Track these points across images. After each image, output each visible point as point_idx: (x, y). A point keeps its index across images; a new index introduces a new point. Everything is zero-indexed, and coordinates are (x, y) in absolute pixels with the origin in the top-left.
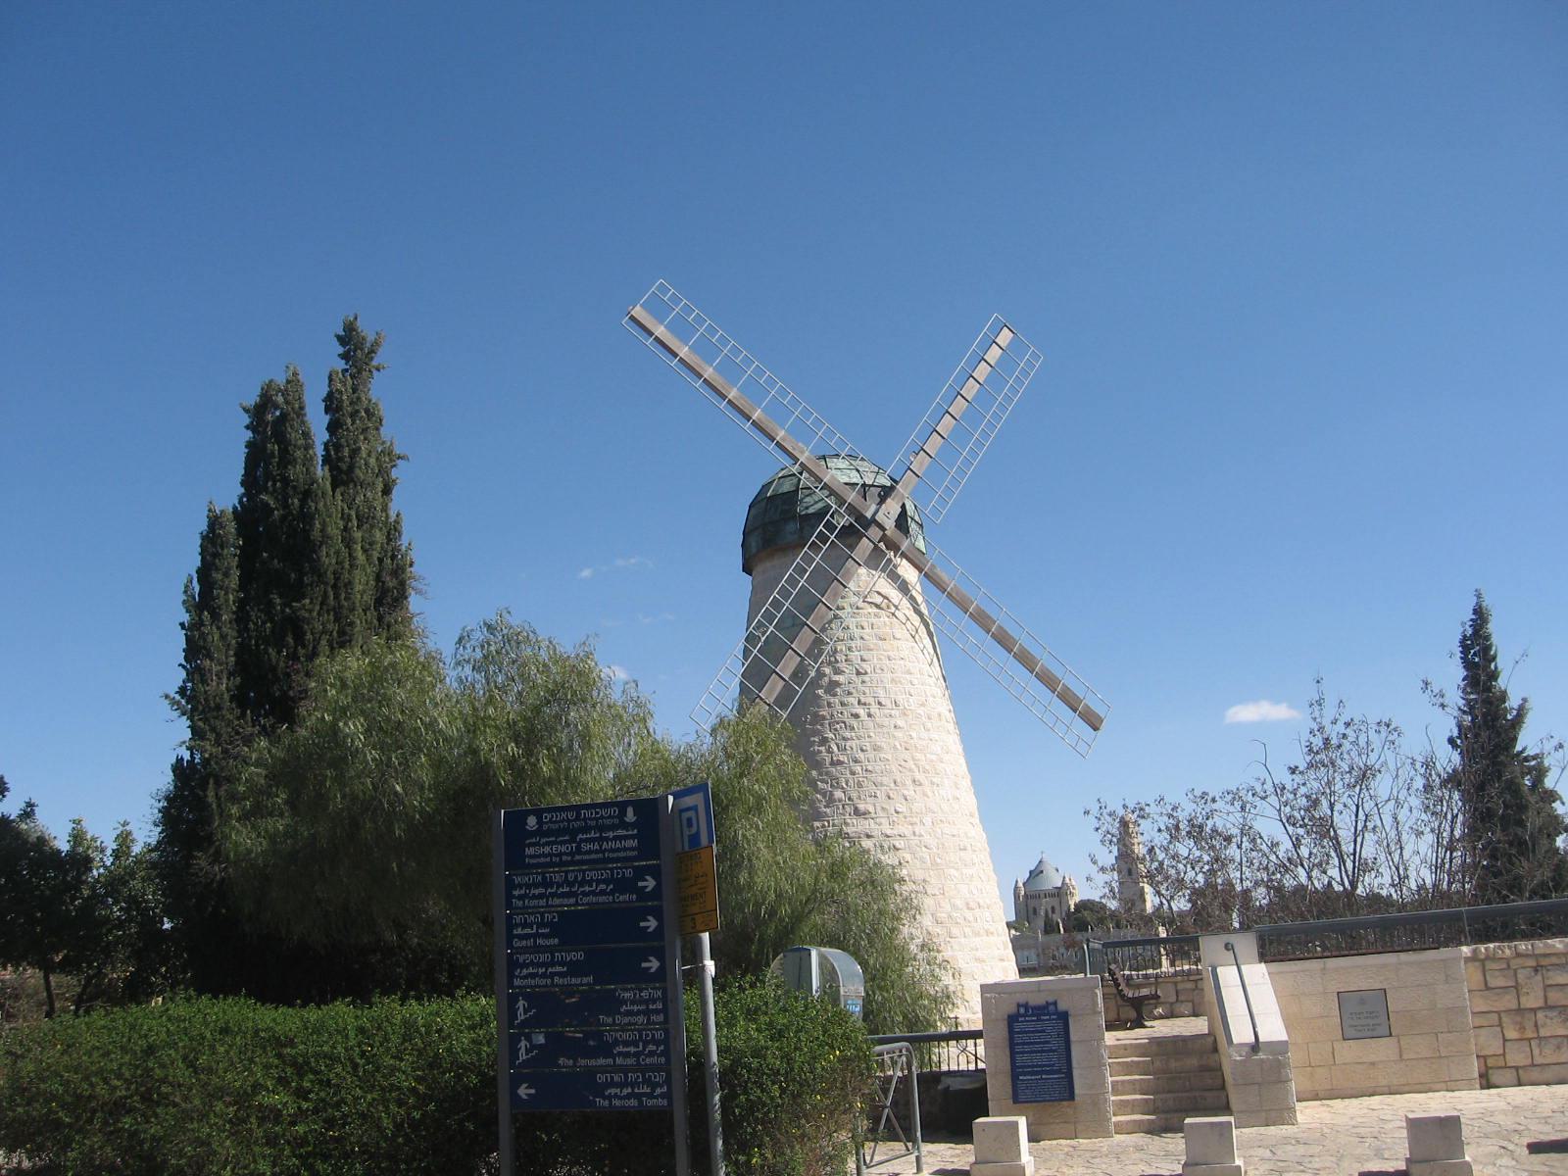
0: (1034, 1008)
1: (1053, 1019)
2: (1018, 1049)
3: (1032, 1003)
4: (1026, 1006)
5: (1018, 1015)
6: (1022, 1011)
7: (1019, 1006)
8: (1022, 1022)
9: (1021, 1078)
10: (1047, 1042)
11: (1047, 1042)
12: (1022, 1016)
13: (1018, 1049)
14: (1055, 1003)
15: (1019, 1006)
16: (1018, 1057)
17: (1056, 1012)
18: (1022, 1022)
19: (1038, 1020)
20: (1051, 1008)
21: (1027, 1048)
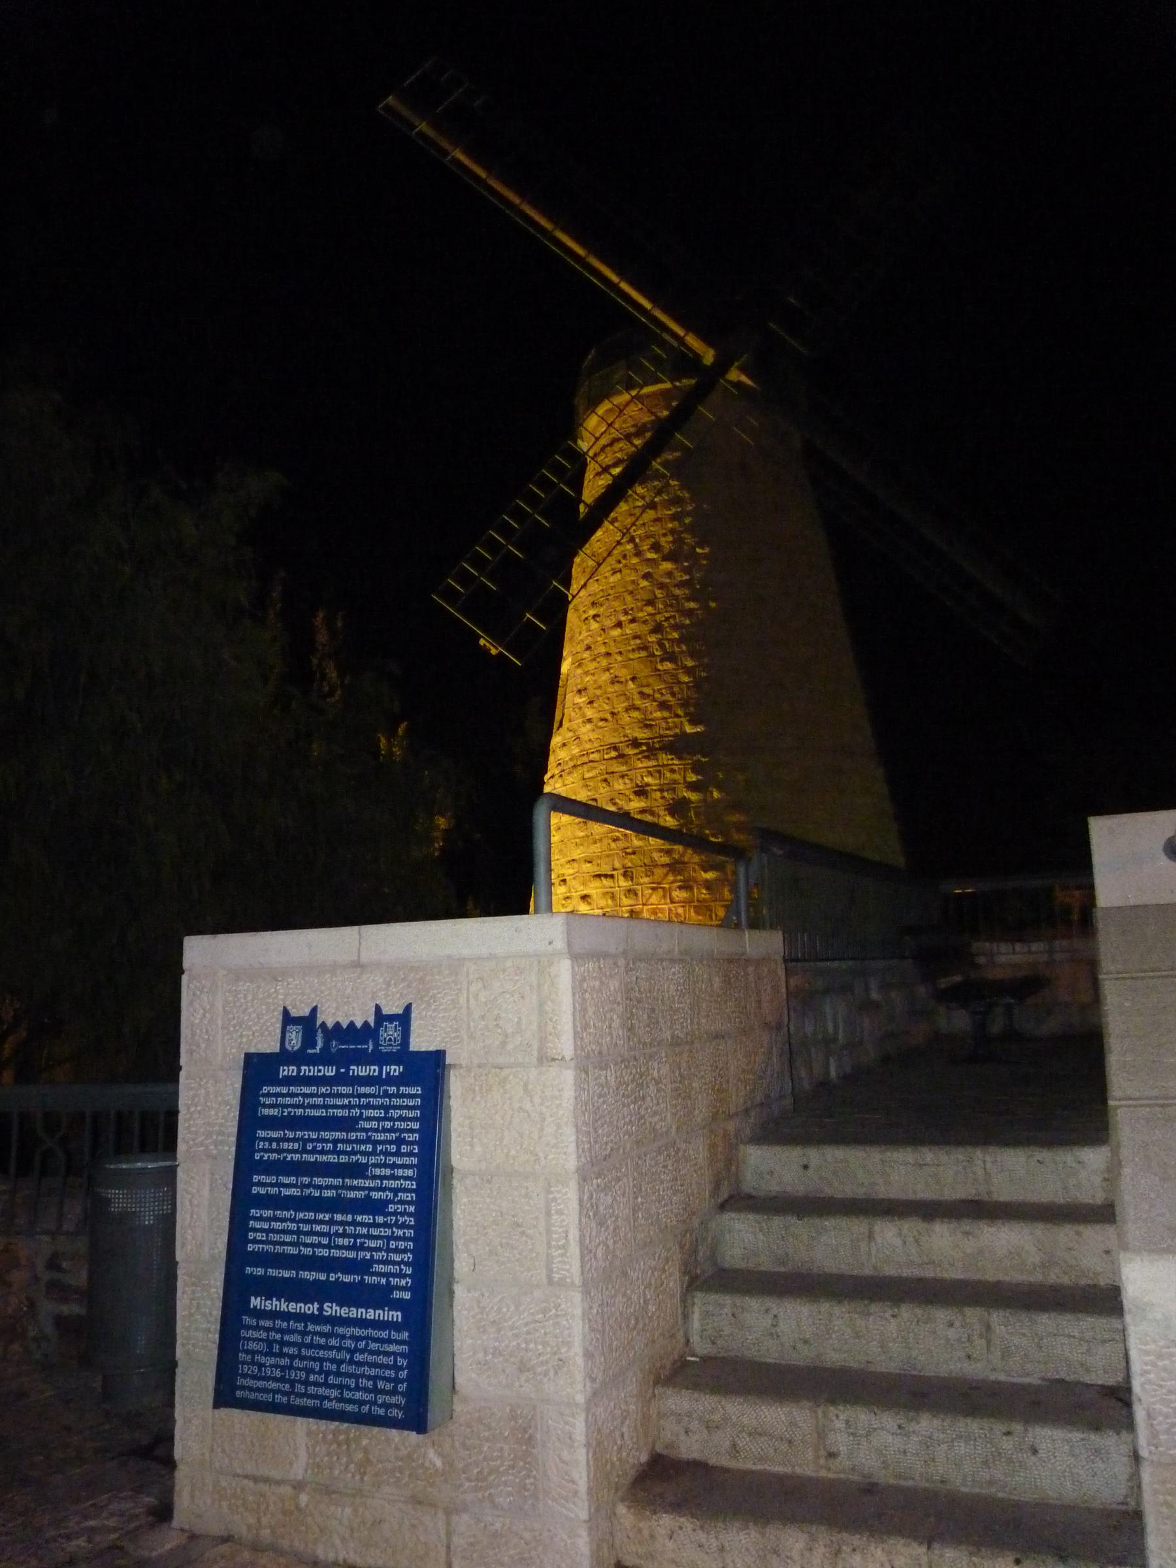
0: (337, 1032)
1: (390, 1080)
2: (262, 1185)
3: (328, 1017)
4: (308, 1023)
5: (284, 1056)
6: (295, 1040)
7: (288, 1019)
8: (289, 1081)
9: (255, 1302)
10: (358, 1171)
11: (358, 1171)
12: (298, 1058)
13: (262, 1185)
14: (404, 1019)
15: (288, 1019)
16: (260, 1220)
17: (403, 1055)
18: (289, 1081)
19: (340, 1079)
20: (390, 1032)
21: (291, 1185)
